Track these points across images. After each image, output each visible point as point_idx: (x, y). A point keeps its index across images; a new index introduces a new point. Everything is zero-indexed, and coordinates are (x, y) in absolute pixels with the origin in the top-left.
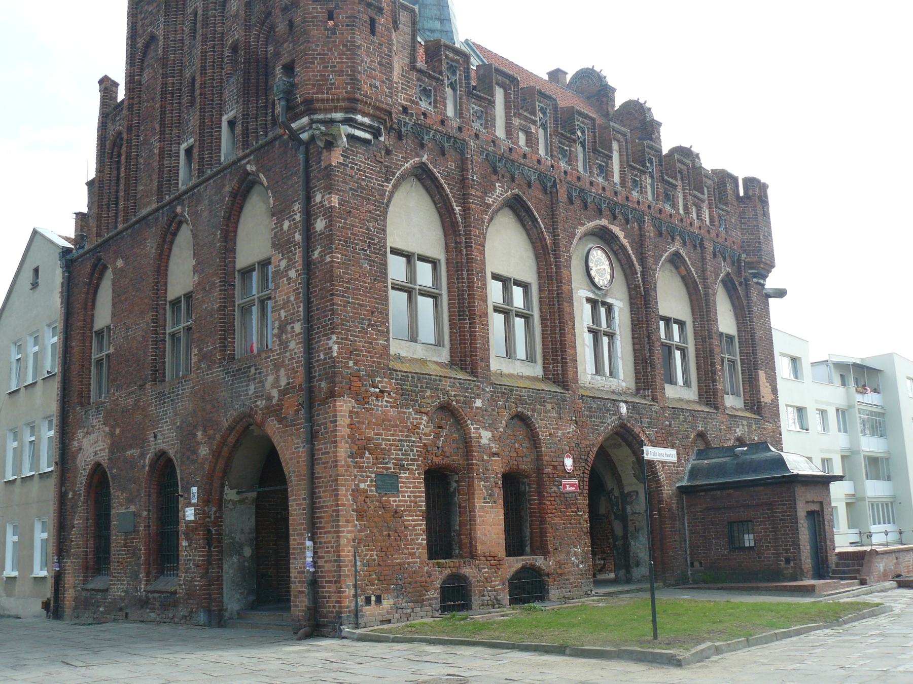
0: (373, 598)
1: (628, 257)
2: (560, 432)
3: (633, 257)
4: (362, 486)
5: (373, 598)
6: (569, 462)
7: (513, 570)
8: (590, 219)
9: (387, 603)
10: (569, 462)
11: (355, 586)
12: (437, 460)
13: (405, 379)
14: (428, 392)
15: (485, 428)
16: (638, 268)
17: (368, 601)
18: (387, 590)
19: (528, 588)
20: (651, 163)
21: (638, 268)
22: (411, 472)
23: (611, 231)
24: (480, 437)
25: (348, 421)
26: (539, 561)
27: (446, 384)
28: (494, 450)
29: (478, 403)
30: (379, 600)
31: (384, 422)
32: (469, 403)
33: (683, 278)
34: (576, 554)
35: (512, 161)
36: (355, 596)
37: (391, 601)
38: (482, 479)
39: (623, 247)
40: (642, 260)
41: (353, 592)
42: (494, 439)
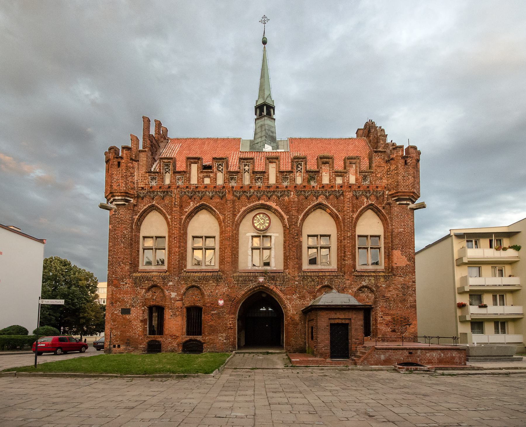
0: (117, 346)
1: (280, 213)
2: (217, 291)
3: (282, 213)
4: (115, 312)
5: (117, 346)
6: (221, 302)
7: (184, 340)
8: (250, 203)
9: (122, 347)
10: (221, 302)
11: (110, 342)
12: (152, 303)
13: (136, 278)
14: (146, 282)
15: (173, 292)
16: (286, 217)
17: (114, 346)
18: (123, 344)
19: (192, 347)
20: (301, 165)
21: (286, 217)
22: (136, 308)
23: (266, 205)
24: (170, 294)
25: (111, 293)
26: (199, 338)
27: (155, 279)
28: (178, 299)
29: (171, 283)
30: (119, 346)
31: (126, 293)
32: (165, 284)
33: (330, 214)
34: (222, 336)
35: (199, 192)
36: (110, 345)
37: (124, 347)
38: (171, 309)
39: (276, 210)
40: (287, 213)
41: (109, 343)
42: (178, 295)
